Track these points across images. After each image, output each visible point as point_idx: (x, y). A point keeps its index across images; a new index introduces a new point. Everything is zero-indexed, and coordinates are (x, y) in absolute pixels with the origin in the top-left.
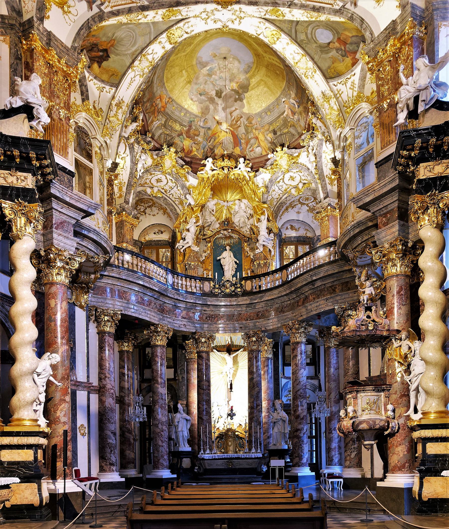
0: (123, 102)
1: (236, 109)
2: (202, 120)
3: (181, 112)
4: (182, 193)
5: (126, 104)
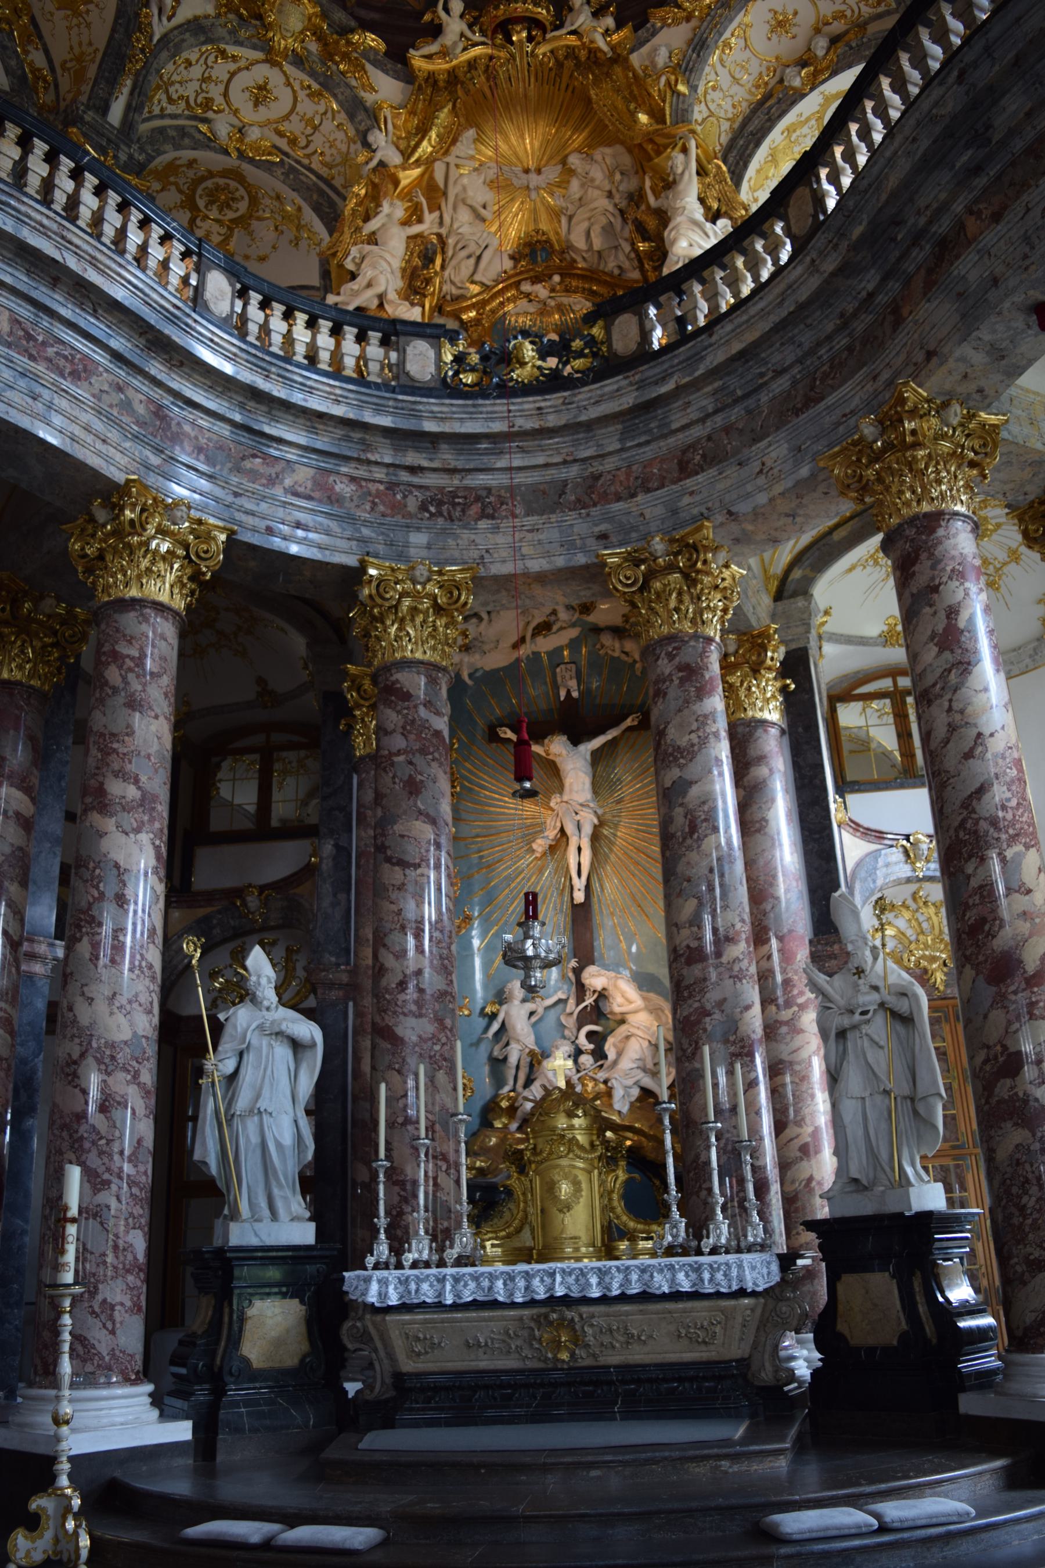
4: (352, 132)
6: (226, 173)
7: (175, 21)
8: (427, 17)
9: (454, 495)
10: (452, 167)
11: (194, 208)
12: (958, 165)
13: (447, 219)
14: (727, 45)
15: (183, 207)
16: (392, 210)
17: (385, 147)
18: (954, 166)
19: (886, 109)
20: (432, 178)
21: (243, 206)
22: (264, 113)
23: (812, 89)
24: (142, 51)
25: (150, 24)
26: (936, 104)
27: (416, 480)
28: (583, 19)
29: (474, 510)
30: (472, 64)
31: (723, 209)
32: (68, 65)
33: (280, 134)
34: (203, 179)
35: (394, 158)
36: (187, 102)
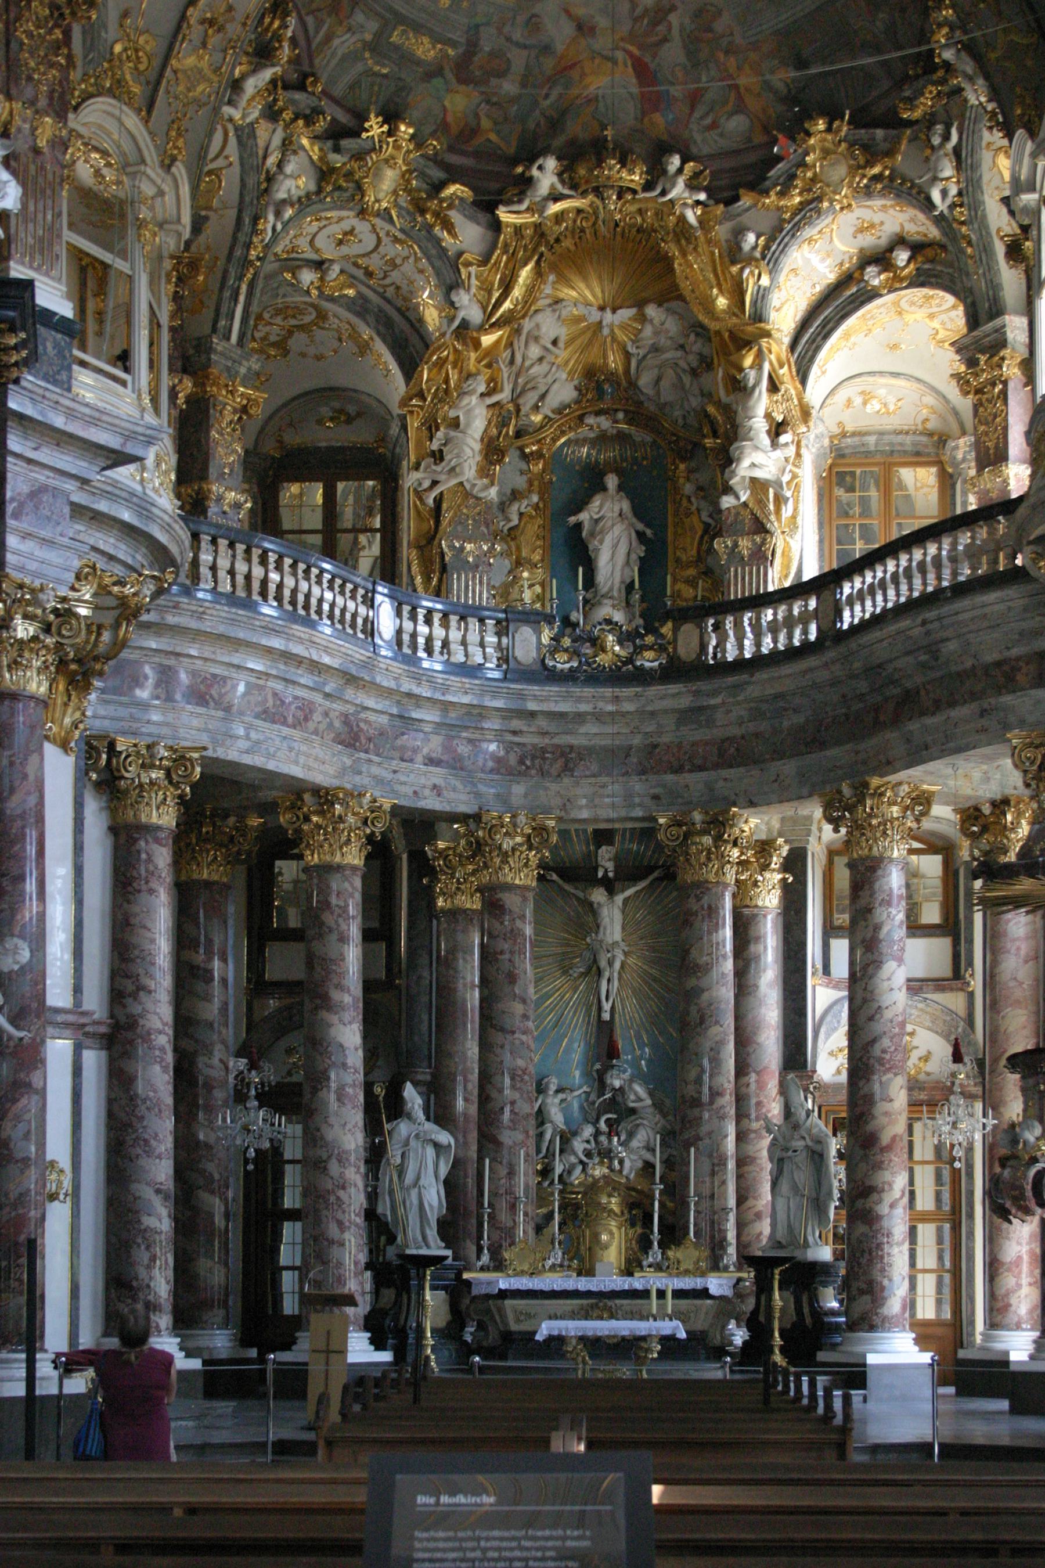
0: (230, 9)
9: (543, 750)
27: (517, 739)
29: (559, 764)
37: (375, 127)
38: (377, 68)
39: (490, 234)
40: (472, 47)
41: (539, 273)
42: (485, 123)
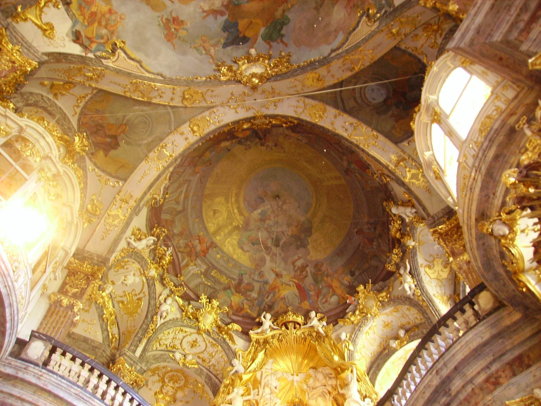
0: (131, 196)
1: (299, 258)
2: (257, 273)
3: (228, 262)
5: (134, 199)
6: (177, 371)
7: (166, 320)
8: (257, 320)
10: (264, 373)
11: (163, 382)
12: (441, 402)
13: (261, 393)
14: (367, 332)
15: (159, 381)
16: (239, 390)
17: (238, 365)
18: (439, 402)
19: (414, 378)
20: (255, 377)
21: (182, 383)
22: (194, 350)
23: (400, 348)
24: (152, 330)
25: (157, 321)
26: (430, 381)
28: (315, 322)
30: (273, 337)
31: (368, 395)
32: (125, 333)
33: (199, 357)
34: (168, 372)
35: (241, 369)
36: (166, 346)
37: (204, 299)
38: (206, 282)
39: (247, 344)
40: (241, 281)
41: (265, 354)
42: (246, 306)
